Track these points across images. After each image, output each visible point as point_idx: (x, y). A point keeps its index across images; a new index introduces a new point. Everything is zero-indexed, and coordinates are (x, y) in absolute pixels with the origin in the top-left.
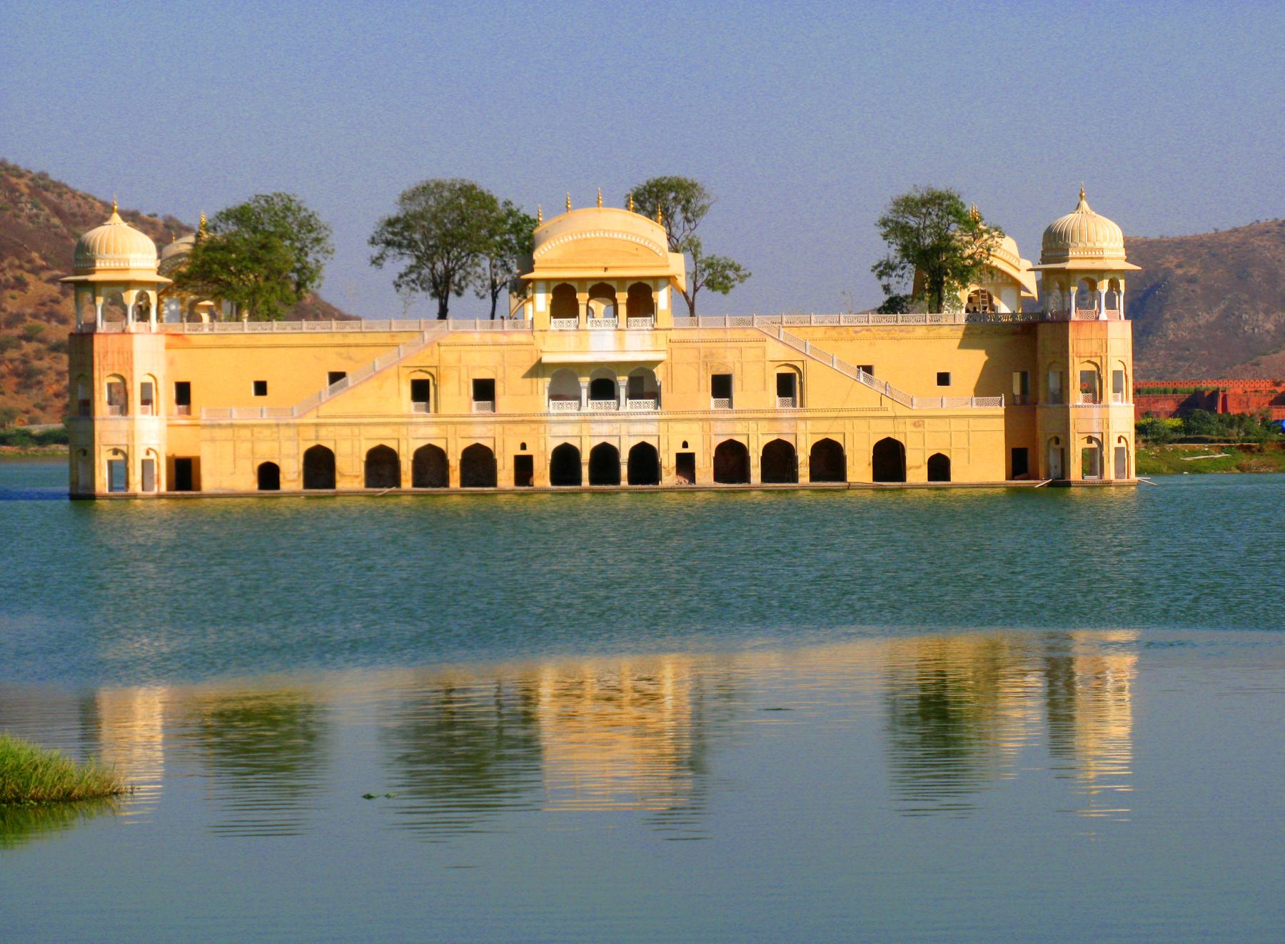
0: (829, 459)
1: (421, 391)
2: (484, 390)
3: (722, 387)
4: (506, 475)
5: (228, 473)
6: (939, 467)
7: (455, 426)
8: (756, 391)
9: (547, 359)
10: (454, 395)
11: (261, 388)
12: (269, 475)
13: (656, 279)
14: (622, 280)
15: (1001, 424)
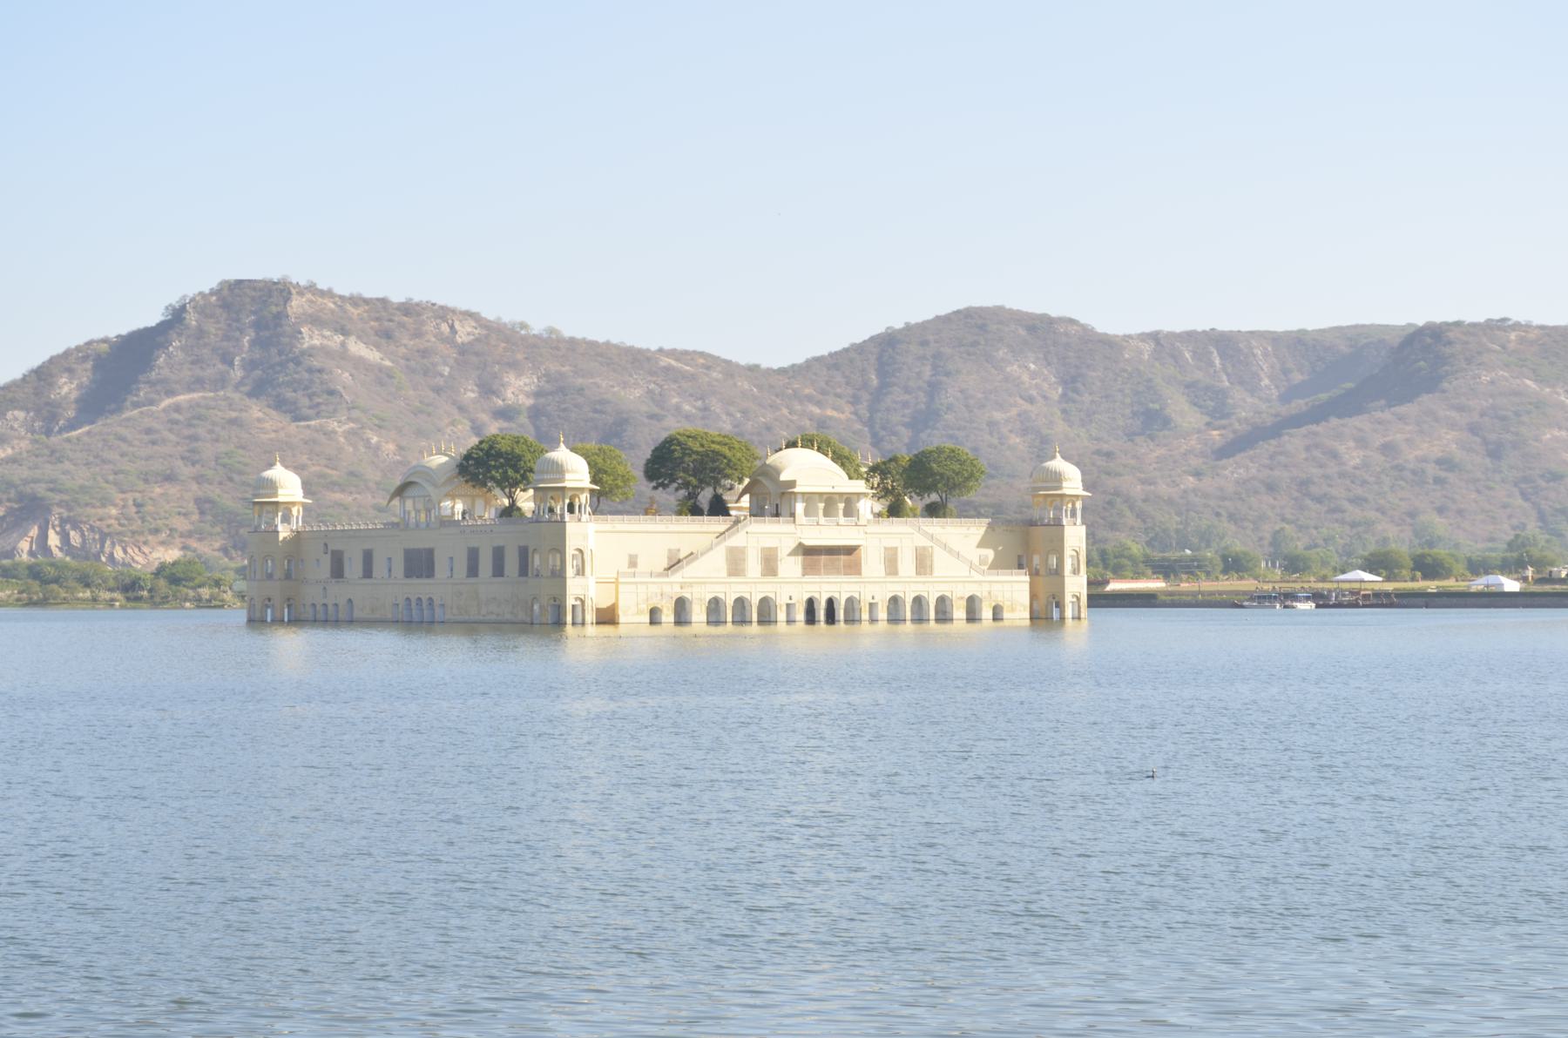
0: (943, 604)
1: (736, 565)
2: (770, 565)
3: (891, 565)
4: (782, 616)
5: (632, 616)
6: (997, 614)
7: (753, 588)
8: (907, 565)
9: (808, 543)
10: (754, 566)
11: (633, 563)
12: (654, 616)
13: (858, 494)
14: (841, 494)
15: (1027, 587)
